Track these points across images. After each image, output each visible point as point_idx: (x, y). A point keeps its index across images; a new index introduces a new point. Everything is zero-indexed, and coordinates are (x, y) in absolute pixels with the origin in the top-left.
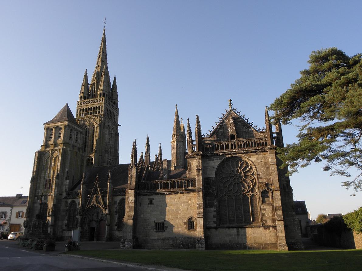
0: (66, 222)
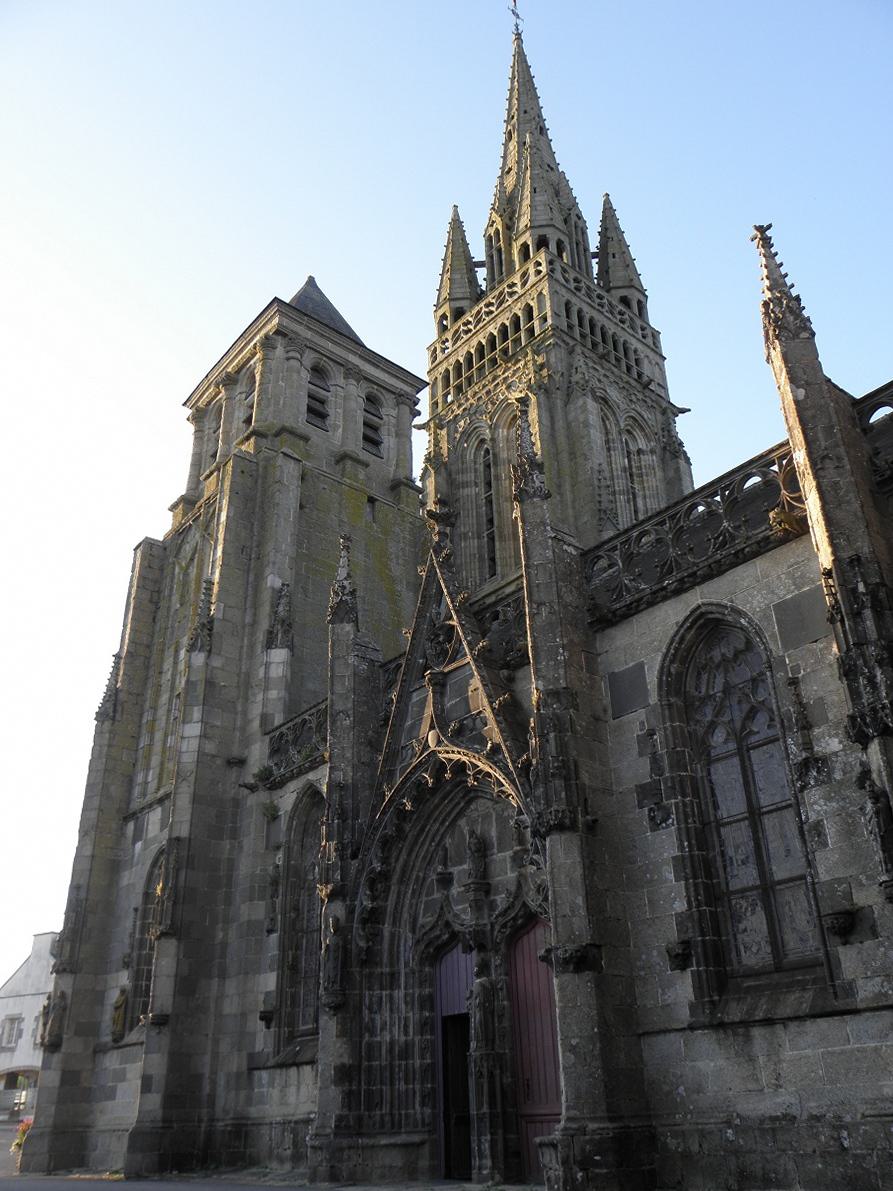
0: (269, 981)
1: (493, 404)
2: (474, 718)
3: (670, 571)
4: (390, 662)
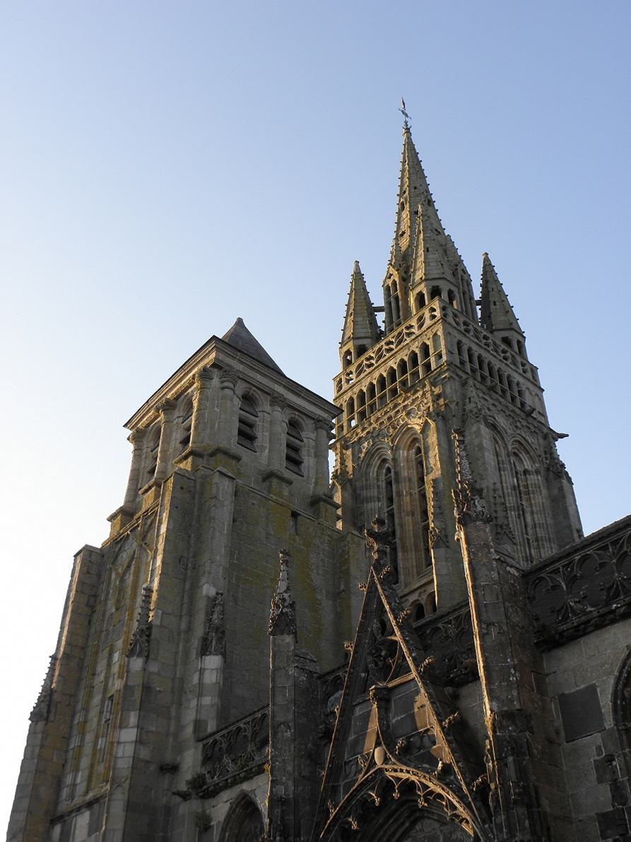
1: (394, 428)
2: (422, 736)
3: (617, 595)
4: (328, 673)
